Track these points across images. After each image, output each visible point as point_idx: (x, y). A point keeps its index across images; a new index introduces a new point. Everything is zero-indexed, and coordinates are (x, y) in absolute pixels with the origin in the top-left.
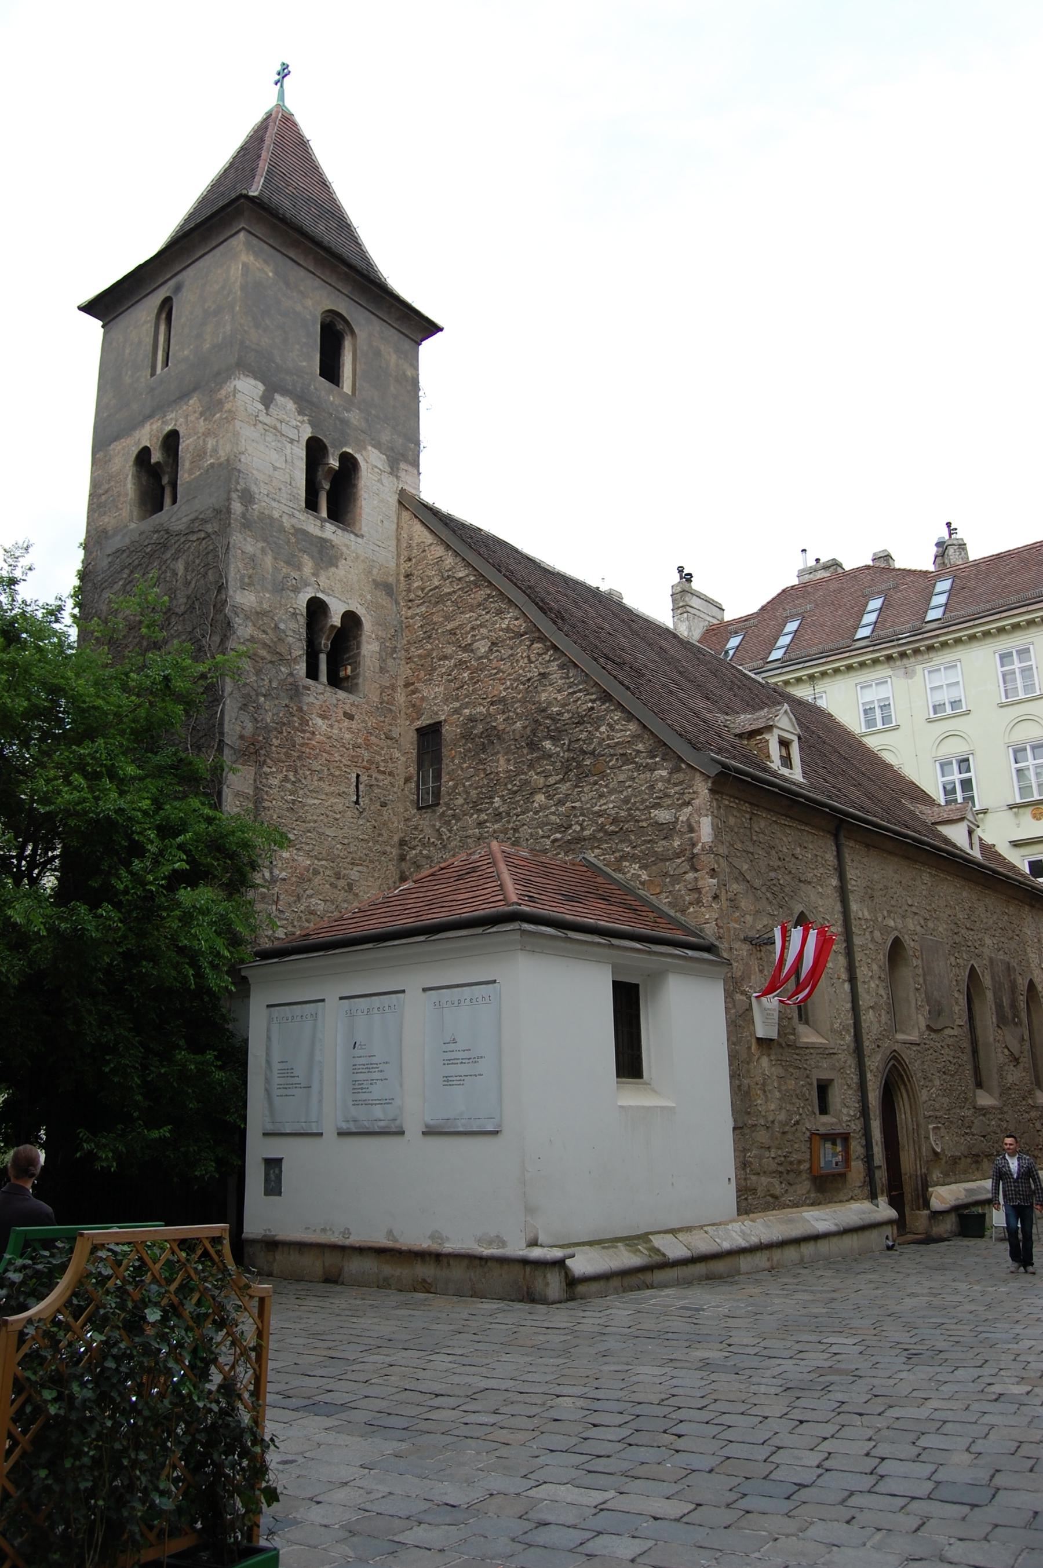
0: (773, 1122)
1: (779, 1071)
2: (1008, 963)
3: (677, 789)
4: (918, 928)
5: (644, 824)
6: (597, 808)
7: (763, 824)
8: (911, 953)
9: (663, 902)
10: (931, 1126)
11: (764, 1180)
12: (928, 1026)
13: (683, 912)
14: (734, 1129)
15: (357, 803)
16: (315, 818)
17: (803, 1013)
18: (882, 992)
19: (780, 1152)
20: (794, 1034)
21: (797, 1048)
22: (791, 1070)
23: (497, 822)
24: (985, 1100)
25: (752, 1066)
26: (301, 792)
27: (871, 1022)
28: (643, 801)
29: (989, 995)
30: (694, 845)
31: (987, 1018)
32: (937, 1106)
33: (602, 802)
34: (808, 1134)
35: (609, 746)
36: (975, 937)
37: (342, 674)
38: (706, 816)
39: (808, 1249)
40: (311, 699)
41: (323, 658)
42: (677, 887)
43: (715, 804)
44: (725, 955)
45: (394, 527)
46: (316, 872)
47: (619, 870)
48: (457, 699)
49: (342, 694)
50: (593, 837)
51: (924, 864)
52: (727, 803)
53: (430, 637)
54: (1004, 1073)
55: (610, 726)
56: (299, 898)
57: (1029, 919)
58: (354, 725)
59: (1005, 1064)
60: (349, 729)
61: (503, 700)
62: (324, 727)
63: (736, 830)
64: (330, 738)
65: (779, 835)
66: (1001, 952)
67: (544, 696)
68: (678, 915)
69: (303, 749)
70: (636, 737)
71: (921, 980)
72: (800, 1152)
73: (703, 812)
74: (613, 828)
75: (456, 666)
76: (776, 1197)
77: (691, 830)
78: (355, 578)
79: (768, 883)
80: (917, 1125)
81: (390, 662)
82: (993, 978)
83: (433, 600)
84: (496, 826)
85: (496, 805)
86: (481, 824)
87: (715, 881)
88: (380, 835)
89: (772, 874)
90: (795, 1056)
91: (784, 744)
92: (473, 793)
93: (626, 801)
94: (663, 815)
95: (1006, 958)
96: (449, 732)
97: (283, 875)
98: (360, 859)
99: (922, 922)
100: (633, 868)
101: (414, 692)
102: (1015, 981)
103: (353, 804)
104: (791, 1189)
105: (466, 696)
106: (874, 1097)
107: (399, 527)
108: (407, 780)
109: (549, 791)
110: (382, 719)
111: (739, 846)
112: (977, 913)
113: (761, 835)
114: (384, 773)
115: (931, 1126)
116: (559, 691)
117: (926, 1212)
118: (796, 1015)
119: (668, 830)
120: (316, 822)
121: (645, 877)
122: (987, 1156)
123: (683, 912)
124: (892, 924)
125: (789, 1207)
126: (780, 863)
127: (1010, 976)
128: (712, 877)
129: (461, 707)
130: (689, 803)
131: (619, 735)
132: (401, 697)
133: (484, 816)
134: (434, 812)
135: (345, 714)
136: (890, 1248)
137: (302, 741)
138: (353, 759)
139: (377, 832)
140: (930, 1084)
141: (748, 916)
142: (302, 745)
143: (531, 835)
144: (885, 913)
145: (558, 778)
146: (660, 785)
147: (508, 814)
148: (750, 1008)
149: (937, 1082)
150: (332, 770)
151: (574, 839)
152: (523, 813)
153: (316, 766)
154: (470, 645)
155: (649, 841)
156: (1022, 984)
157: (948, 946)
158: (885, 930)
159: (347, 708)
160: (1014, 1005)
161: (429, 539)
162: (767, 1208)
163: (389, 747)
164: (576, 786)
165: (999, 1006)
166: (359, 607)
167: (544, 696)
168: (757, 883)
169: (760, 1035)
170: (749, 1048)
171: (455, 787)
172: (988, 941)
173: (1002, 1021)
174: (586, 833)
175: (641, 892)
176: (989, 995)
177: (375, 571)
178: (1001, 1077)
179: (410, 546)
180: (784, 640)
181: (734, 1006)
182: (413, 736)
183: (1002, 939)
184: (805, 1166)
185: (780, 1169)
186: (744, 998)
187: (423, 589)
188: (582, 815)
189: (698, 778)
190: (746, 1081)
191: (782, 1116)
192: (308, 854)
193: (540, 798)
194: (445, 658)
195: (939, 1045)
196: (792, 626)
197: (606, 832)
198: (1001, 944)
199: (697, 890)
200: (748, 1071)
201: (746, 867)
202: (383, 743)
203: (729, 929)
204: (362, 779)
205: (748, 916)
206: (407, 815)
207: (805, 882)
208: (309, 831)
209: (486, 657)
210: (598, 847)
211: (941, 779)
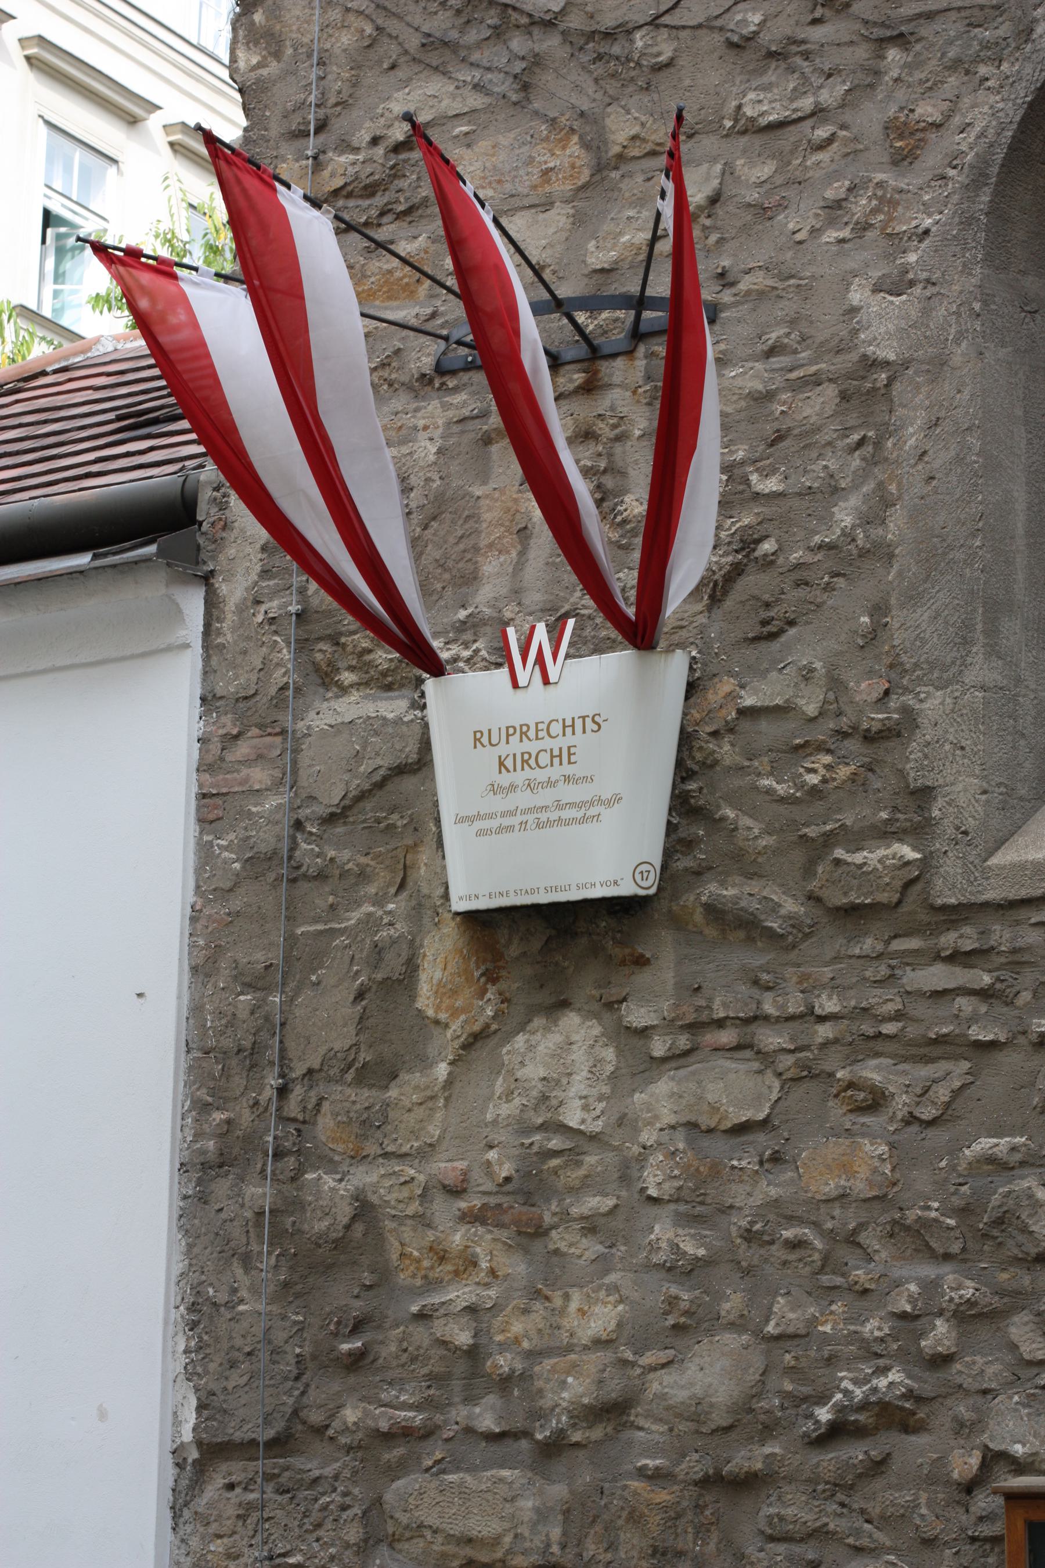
0: (613, 1411)
14: (204, 1459)
20: (918, 831)
21: (955, 915)
25: (403, 1091)
90: (937, 976)
191: (709, 1374)
200: (370, 1124)
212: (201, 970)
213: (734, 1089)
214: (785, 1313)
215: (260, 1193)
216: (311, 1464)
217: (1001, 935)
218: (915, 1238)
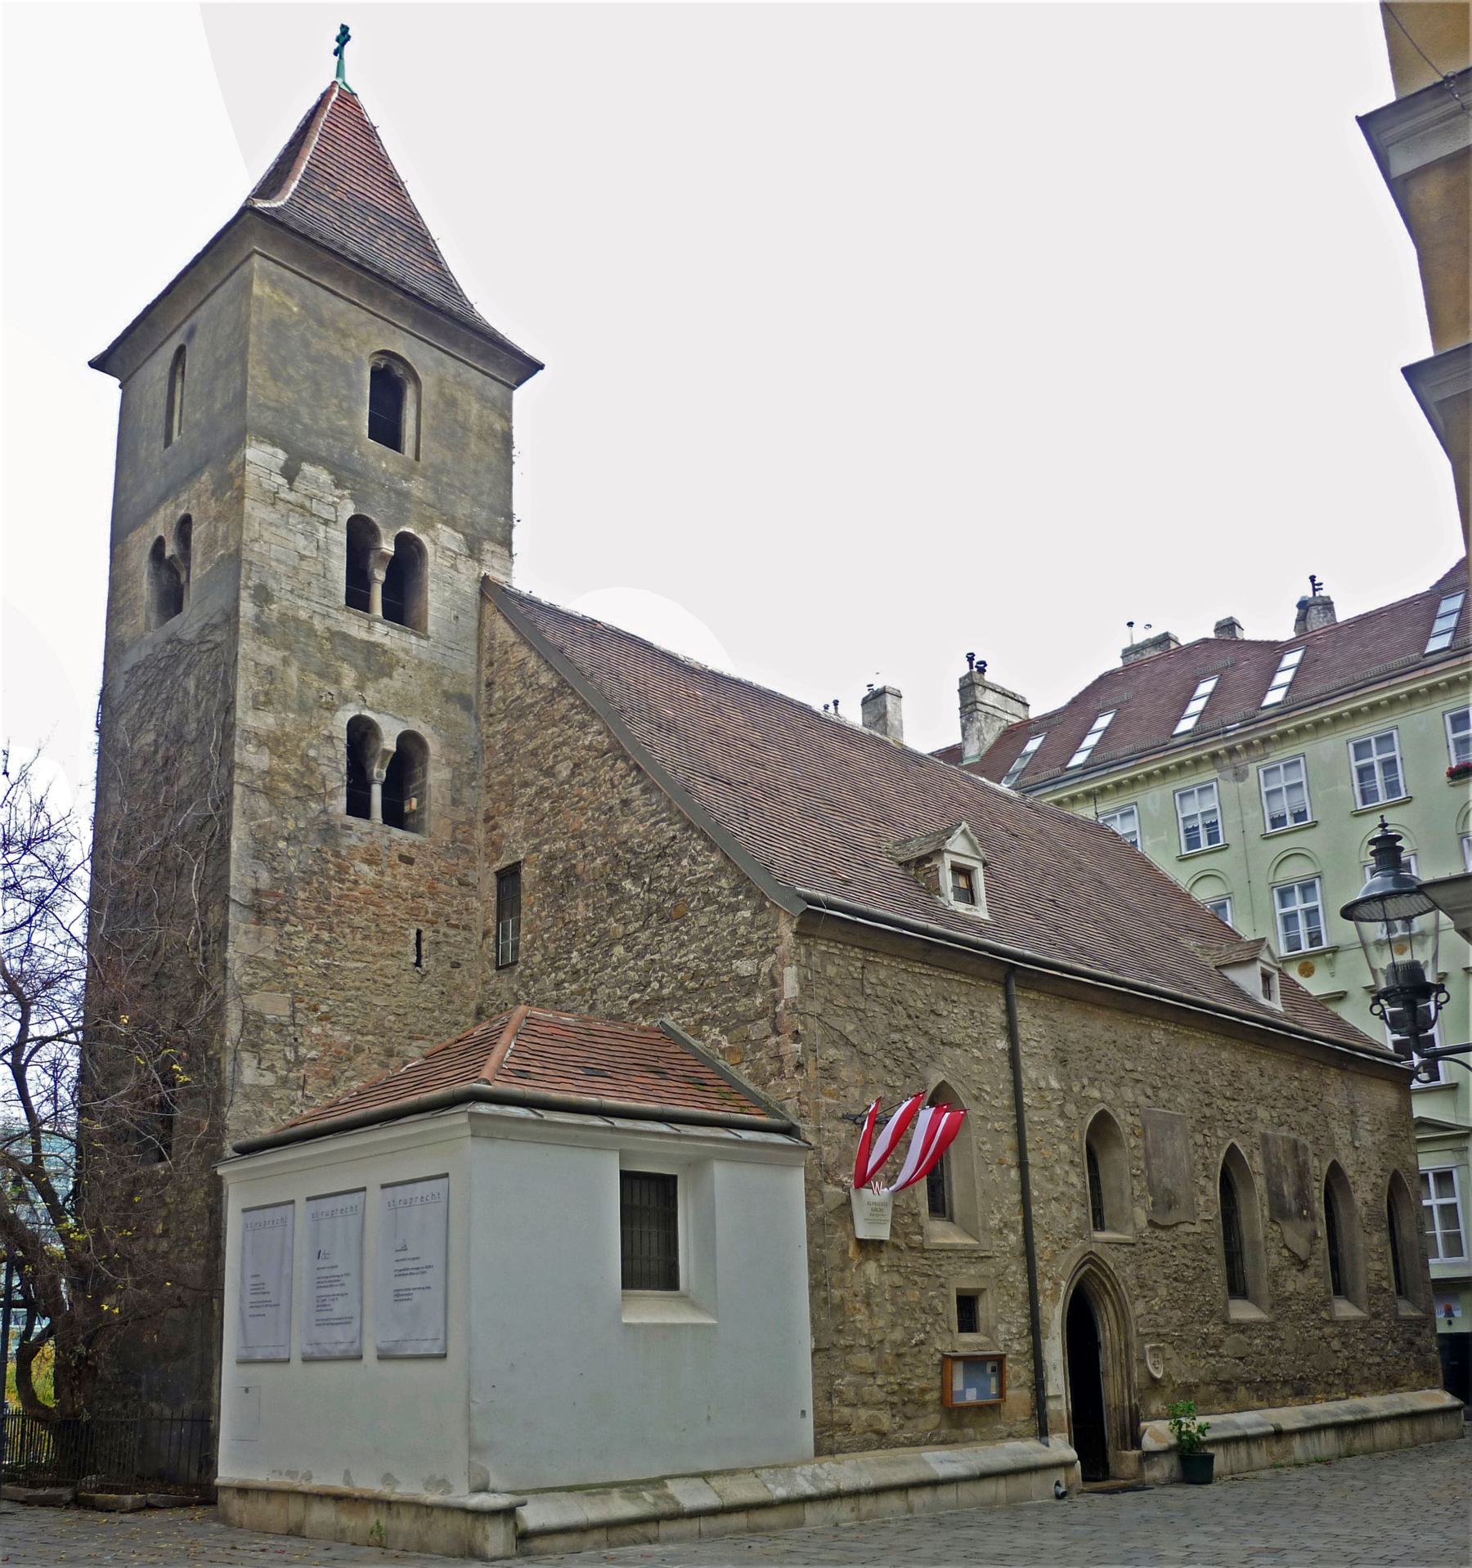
0: (881, 1342)
1: (897, 1279)
2: (1295, 1141)
3: (760, 933)
4: (1142, 1099)
5: (725, 978)
6: (676, 961)
7: (883, 974)
8: (1128, 1130)
9: (743, 1074)
10: (1147, 1346)
11: (863, 1414)
12: (1151, 1223)
13: (764, 1084)
14: (815, 1352)
15: (418, 964)
16: (357, 984)
17: (939, 1206)
18: (1074, 1179)
19: (892, 1379)
20: (921, 1234)
22: (916, 1278)
23: (575, 981)
24: (1242, 1311)
25: (847, 1274)
26: (338, 954)
27: (1054, 1218)
28: (724, 950)
29: (1260, 1183)
30: (776, 1002)
31: (1256, 1210)
32: (1161, 1320)
33: (683, 952)
34: (939, 1356)
35: (690, 884)
36: (1241, 1109)
37: (407, 809)
38: (790, 965)
39: (919, 1498)
40: (353, 841)
41: (377, 791)
42: (758, 1055)
43: (802, 950)
44: (811, 1138)
45: (474, 624)
46: (359, 1050)
47: (699, 1036)
48: (537, 835)
49: (397, 833)
50: (672, 997)
51: (1155, 1018)
52: (823, 948)
53: (511, 759)
54: (1280, 1280)
55: (693, 859)
56: (334, 1081)
57: (1338, 1085)
58: (414, 870)
59: (1283, 1268)
60: (408, 876)
61: (584, 834)
62: (372, 874)
63: (839, 981)
64: (378, 887)
65: (910, 986)
66: (1285, 1128)
67: (625, 829)
68: (759, 1089)
69: (342, 902)
70: (720, 871)
71: (1142, 1165)
72: (924, 1379)
73: (787, 961)
74: (692, 985)
75: (536, 793)
76: (882, 1434)
77: (774, 984)
78: (418, 691)
79: (888, 1048)
80: (1127, 1345)
81: (467, 793)
82: (1267, 1160)
83: (516, 713)
84: (574, 987)
85: (574, 961)
86: (558, 985)
87: (799, 1046)
88: (449, 1002)
89: (896, 1036)
91: (959, 871)
92: (552, 946)
93: (707, 951)
94: (745, 967)
95: (1293, 1135)
96: (528, 874)
97: (313, 1054)
98: (422, 1031)
99: (1149, 1092)
100: (713, 1033)
101: (494, 828)
102: (1305, 1163)
103: (411, 967)
104: (910, 1424)
105: (547, 831)
106: (1054, 1316)
107: (481, 624)
108: (485, 935)
109: (628, 940)
110: (455, 861)
111: (842, 1001)
112: (1244, 1078)
113: (879, 988)
114: (456, 926)
115: (1147, 1346)
116: (641, 822)
117: (1136, 1452)
118: (924, 1210)
119: (748, 985)
120: (359, 989)
121: (725, 1044)
122: (1244, 1383)
123: (764, 1084)
124: (1096, 1094)
125: (903, 1445)
126: (909, 1022)
127: (1297, 1157)
128: (795, 1042)
129: (541, 844)
130: (773, 951)
131: (701, 869)
132: (480, 834)
133: (561, 975)
134: (512, 972)
135: (402, 858)
136: (1060, 1497)
137: (339, 892)
138: (414, 913)
139: (446, 998)
140: (1150, 1293)
141: (852, 1089)
142: (340, 897)
143: (609, 996)
144: (1085, 1081)
145: (637, 925)
146: (742, 930)
147: (586, 971)
148: (849, 1199)
149: (1163, 1292)
150: (383, 926)
151: (653, 999)
152: (601, 969)
153: (358, 921)
154: (552, 767)
155: (730, 999)
156: (1318, 1168)
157: (1192, 1122)
158: (1084, 1102)
159: (404, 851)
160: (1302, 1194)
161: (512, 637)
162: (866, 1446)
163: (463, 896)
164: (655, 934)
165: (1275, 1195)
166: (423, 725)
167: (625, 829)
168: (869, 1047)
169: (860, 1235)
170: (845, 1252)
171: (533, 941)
172: (1262, 1113)
173: (1279, 1213)
174: (665, 991)
175: (721, 1062)
176: (1260, 1183)
177: (446, 681)
178: (1275, 1283)
179: (491, 648)
180: (1091, 740)
181: (822, 1201)
182: (491, 882)
183: (1289, 1111)
184: (934, 1395)
185: (895, 1399)
186: (840, 1190)
187: (504, 701)
188: (662, 969)
189: (783, 919)
190: (837, 1293)
191: (898, 1335)
192: (348, 1029)
193: (619, 950)
194: (526, 784)
195: (1169, 1246)
196: (1103, 722)
197: (686, 990)
198: (1283, 1118)
199: (779, 1058)
200: (842, 1280)
201: (850, 1027)
202: (456, 891)
203: (818, 1106)
204: (424, 935)
205: (852, 1089)
206: (485, 977)
207: (951, 1044)
208: (348, 1000)
209: (568, 782)
210: (677, 1009)
211: (1280, 911)
212: (809, 1242)
213: (897, 1279)
214: (907, 1323)
215: (823, 1294)
216: (834, 1353)
217: (932, 1256)
218: (923, 1311)
